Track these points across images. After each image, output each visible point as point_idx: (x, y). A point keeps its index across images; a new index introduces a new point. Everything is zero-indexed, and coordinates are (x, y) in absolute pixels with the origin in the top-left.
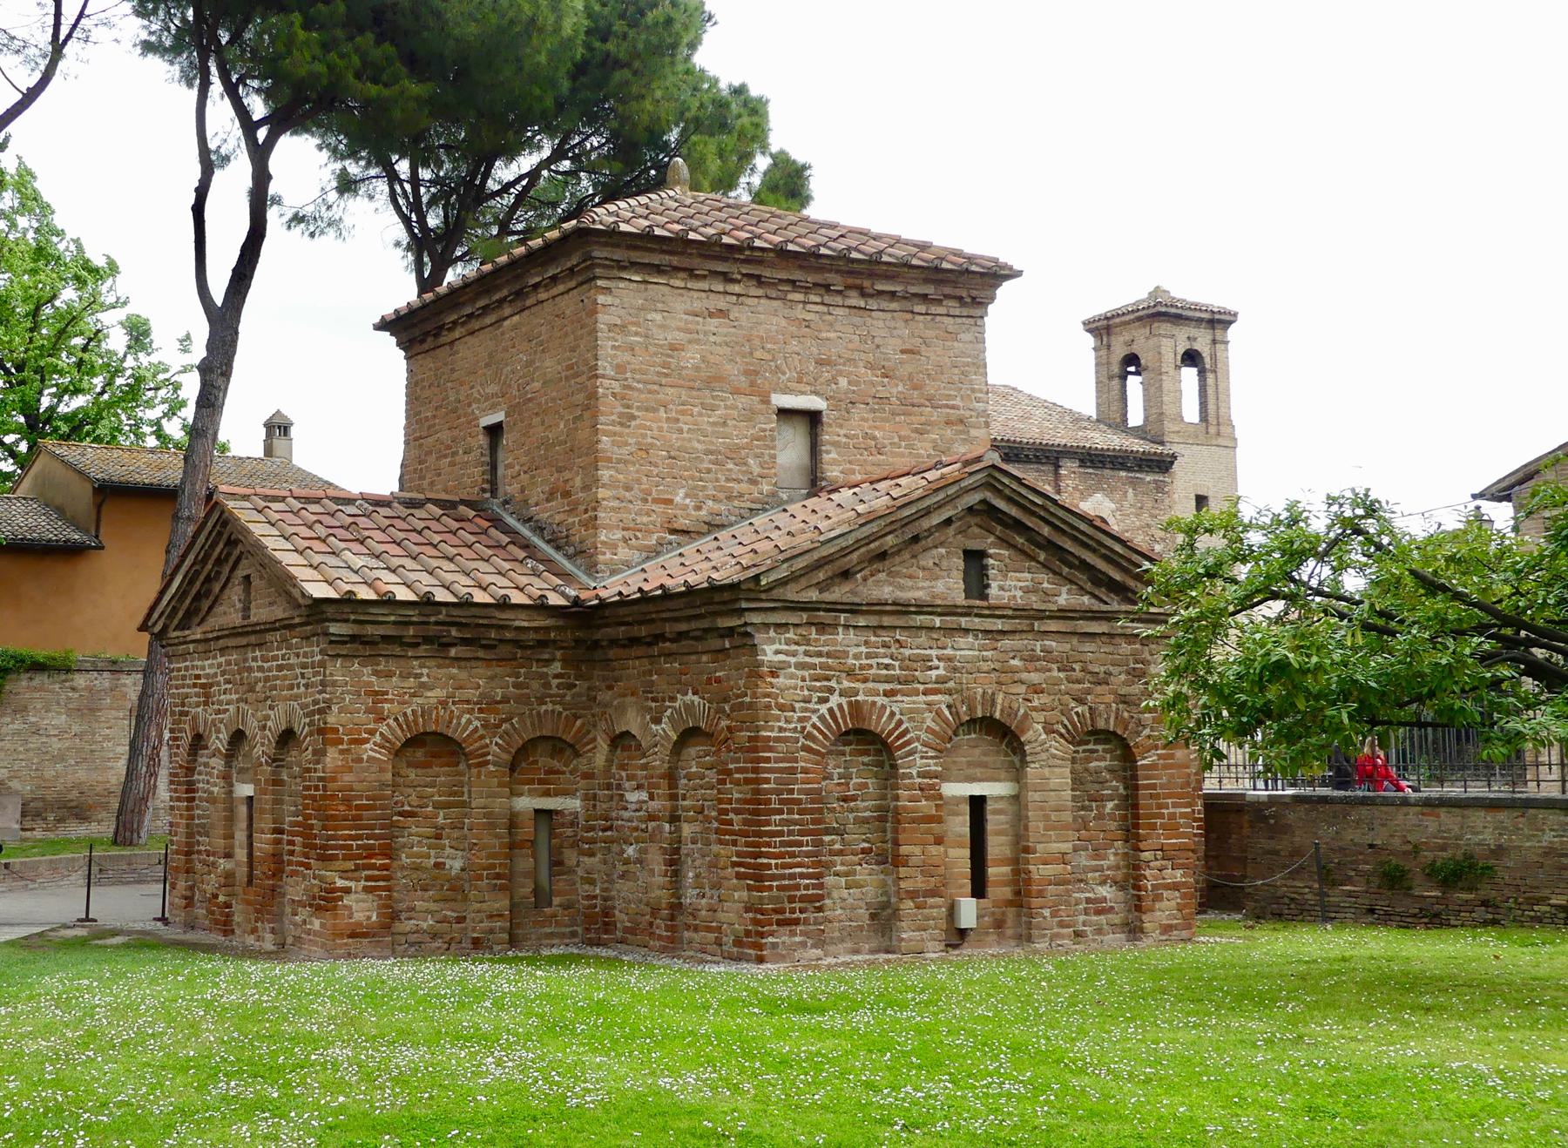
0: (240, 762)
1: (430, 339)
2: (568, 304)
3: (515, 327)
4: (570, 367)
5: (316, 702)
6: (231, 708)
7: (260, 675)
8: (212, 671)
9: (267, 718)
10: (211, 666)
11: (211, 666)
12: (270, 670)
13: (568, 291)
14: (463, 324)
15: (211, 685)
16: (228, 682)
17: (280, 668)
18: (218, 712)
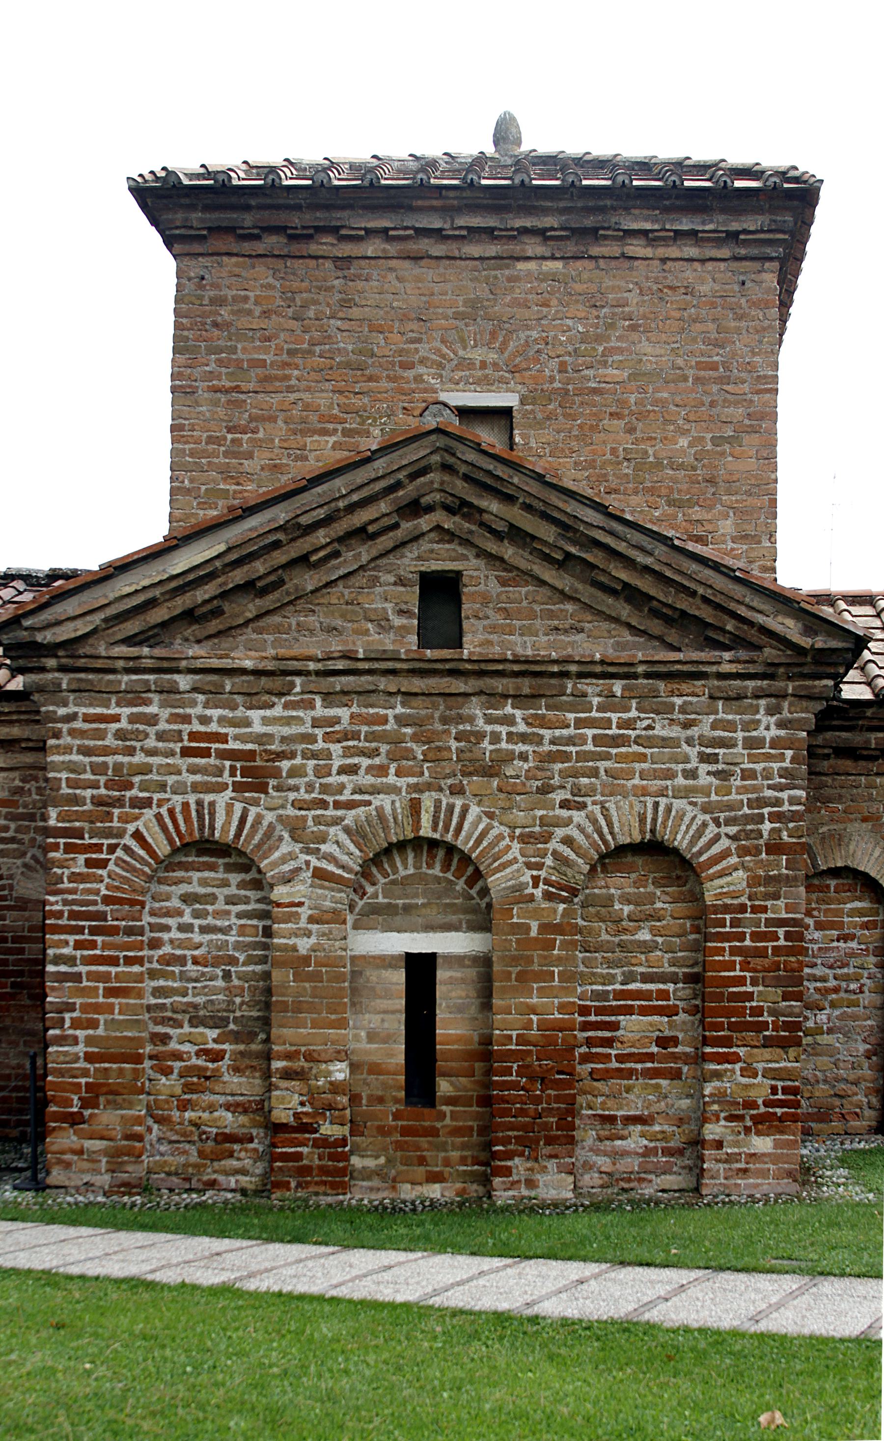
0: (377, 892)
1: (272, 242)
2: (709, 279)
3: (543, 277)
4: (700, 366)
5: (761, 802)
6: (384, 801)
7: (520, 747)
8: (286, 731)
9: (568, 822)
10: (288, 721)
11: (265, 721)
12: (570, 741)
13: (703, 261)
14: (390, 239)
15: (281, 756)
16: (348, 752)
17: (617, 741)
18: (324, 804)
